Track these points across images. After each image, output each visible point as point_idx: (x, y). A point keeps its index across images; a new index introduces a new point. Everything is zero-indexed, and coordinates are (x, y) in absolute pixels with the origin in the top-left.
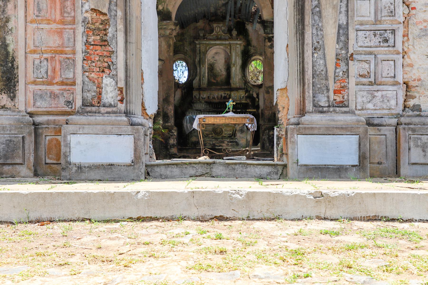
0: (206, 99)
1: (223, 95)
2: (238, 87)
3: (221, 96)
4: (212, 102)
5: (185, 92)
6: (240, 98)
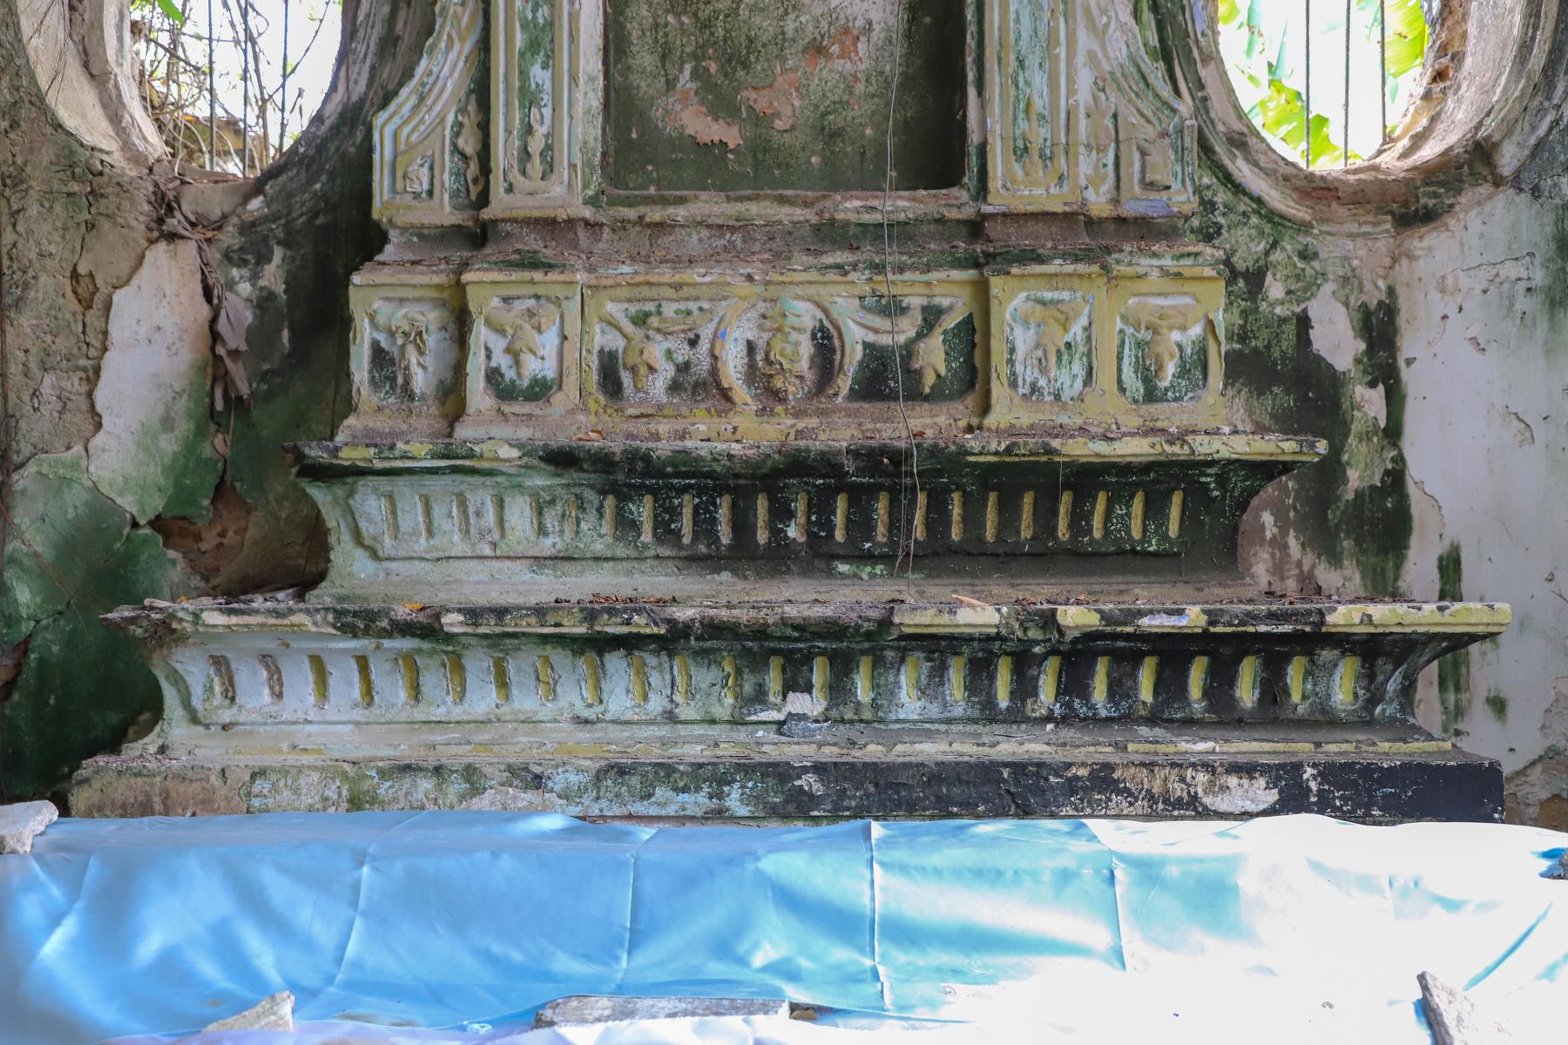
0: (561, 402)
1: (857, 334)
2: (1098, 202)
3: (826, 346)
4: (663, 449)
5: (264, 302)
6: (1149, 379)
